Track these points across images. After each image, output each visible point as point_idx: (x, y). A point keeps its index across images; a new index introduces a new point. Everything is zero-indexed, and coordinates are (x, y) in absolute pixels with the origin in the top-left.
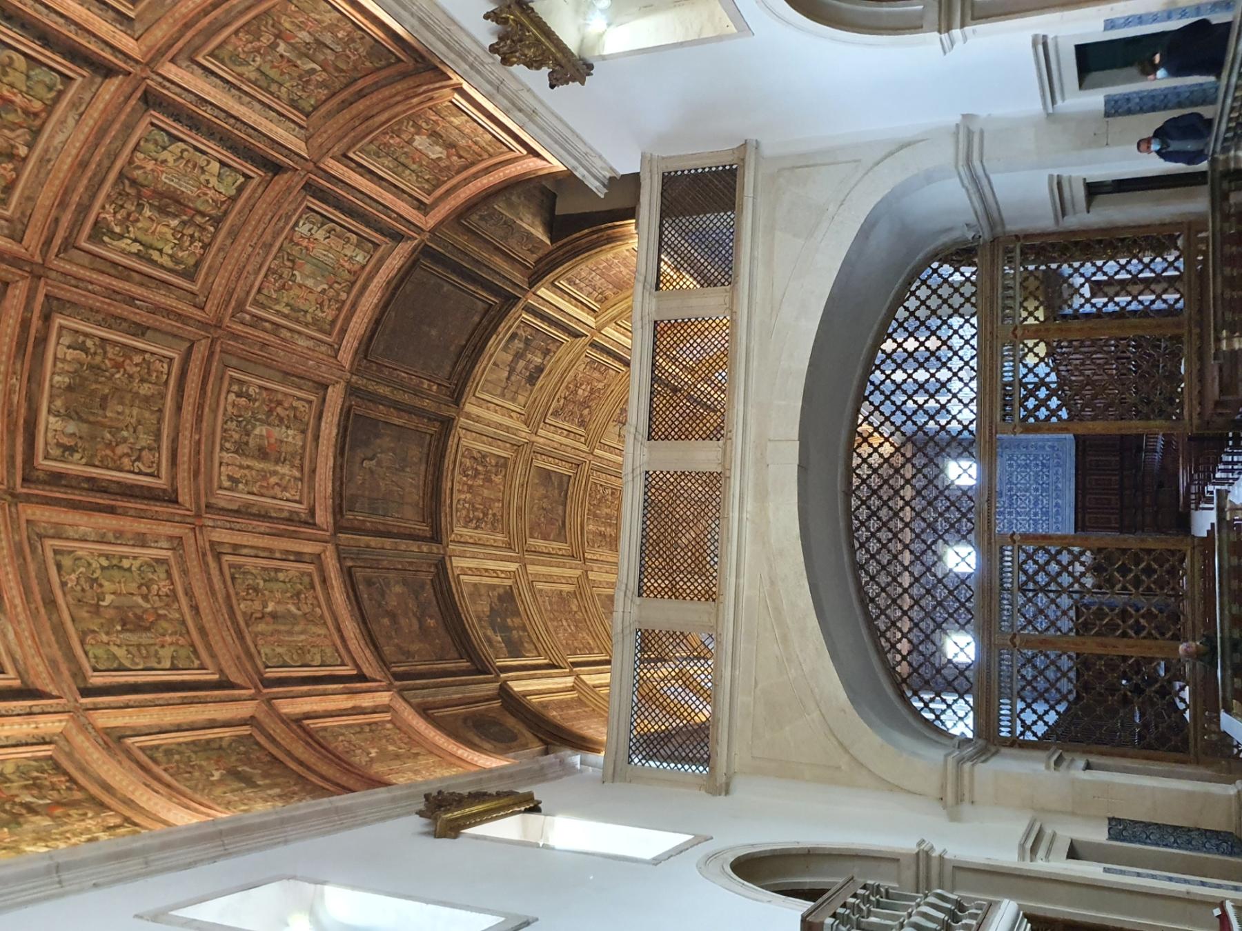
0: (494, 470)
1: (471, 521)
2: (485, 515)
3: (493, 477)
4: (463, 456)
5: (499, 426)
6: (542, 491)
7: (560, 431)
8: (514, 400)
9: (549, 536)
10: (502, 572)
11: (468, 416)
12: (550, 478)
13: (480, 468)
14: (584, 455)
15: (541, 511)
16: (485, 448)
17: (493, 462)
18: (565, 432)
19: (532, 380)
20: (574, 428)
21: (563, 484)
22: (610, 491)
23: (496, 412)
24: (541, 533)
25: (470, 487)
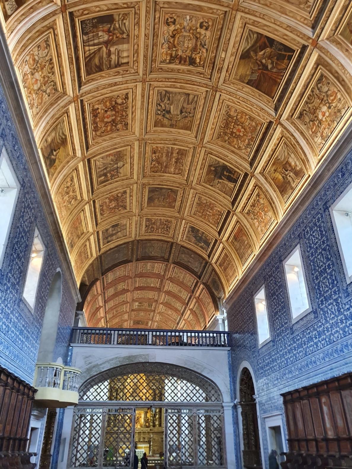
0: (150, 222)
1: (167, 230)
2: (165, 224)
3: (153, 222)
4: (147, 232)
5: (136, 228)
6: (156, 201)
7: (131, 201)
8: (126, 225)
9: (175, 198)
10: (185, 225)
11: (136, 237)
12: (151, 197)
13: (150, 227)
14: (138, 186)
15: (164, 201)
16: (144, 226)
17: (148, 222)
18: (131, 198)
19: (117, 225)
20: (128, 195)
21: (151, 191)
22: (154, 155)
23: (131, 228)
24: (173, 202)
25: (157, 229)
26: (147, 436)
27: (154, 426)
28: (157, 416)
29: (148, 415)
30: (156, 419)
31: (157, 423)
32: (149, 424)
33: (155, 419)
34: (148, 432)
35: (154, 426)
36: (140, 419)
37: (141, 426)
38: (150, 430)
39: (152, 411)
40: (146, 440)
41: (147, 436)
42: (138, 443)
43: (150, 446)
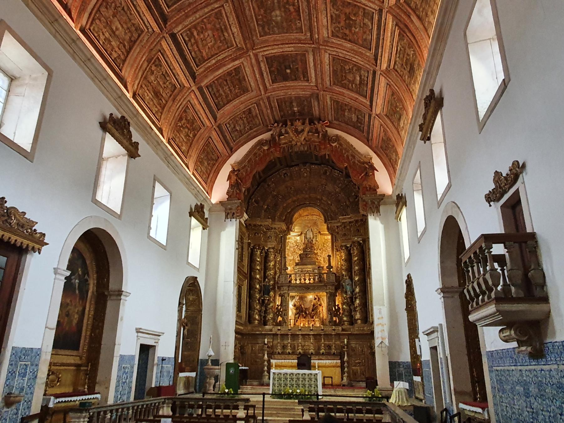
26: (334, 343)
27: (352, 322)
28: (358, 301)
29: (338, 301)
30: (355, 308)
31: (358, 316)
32: (341, 319)
33: (352, 307)
34: (338, 335)
35: (352, 322)
36: (321, 308)
37: (323, 323)
38: (343, 330)
39: (346, 293)
40: (333, 351)
41: (334, 343)
42: (313, 357)
43: (343, 363)
